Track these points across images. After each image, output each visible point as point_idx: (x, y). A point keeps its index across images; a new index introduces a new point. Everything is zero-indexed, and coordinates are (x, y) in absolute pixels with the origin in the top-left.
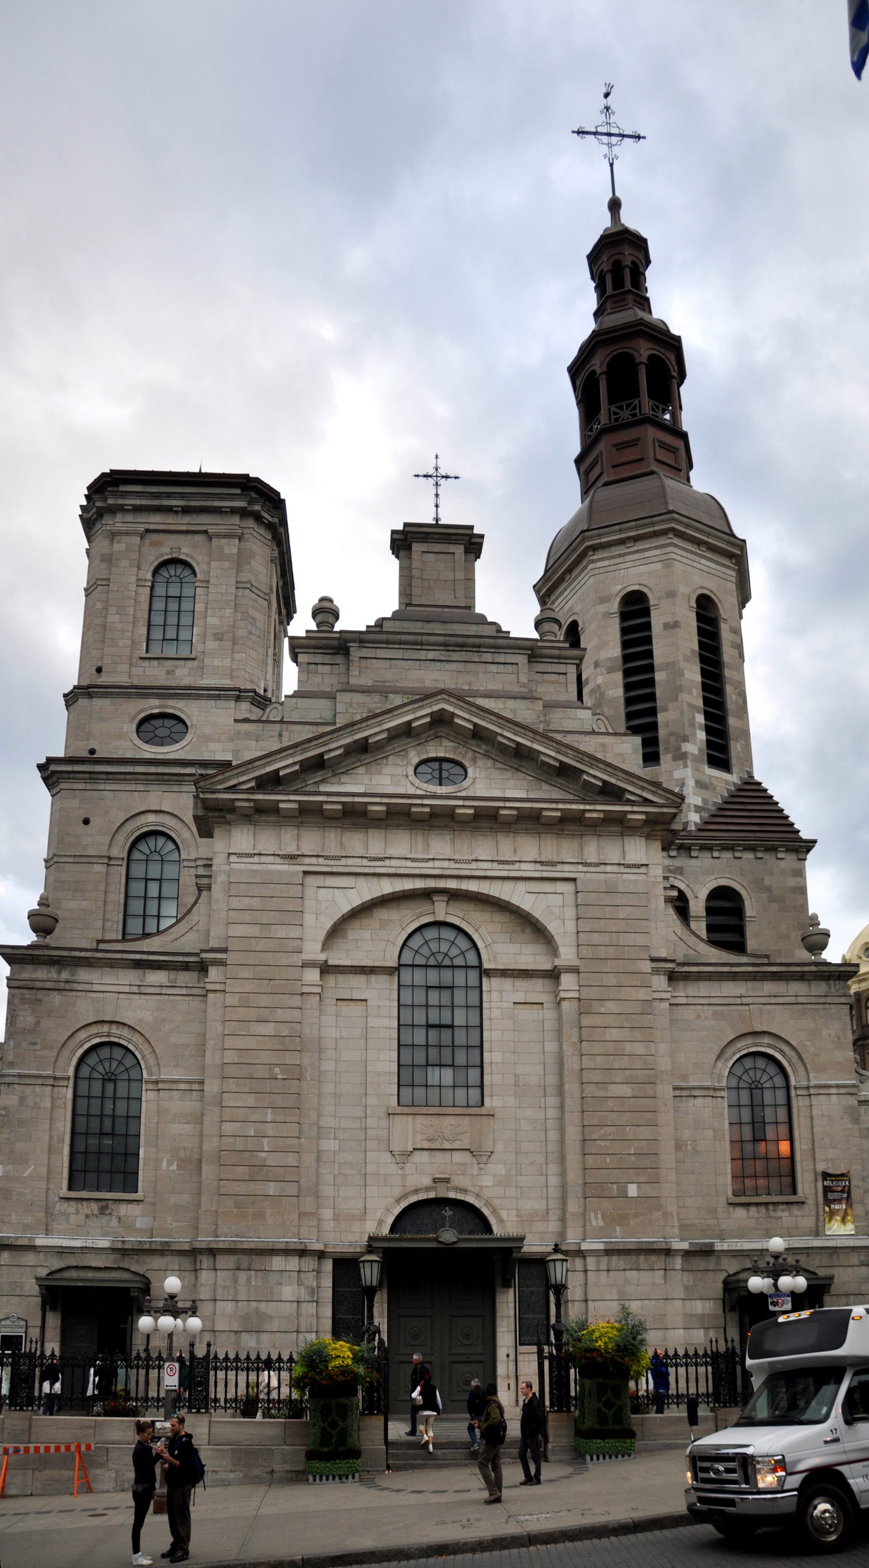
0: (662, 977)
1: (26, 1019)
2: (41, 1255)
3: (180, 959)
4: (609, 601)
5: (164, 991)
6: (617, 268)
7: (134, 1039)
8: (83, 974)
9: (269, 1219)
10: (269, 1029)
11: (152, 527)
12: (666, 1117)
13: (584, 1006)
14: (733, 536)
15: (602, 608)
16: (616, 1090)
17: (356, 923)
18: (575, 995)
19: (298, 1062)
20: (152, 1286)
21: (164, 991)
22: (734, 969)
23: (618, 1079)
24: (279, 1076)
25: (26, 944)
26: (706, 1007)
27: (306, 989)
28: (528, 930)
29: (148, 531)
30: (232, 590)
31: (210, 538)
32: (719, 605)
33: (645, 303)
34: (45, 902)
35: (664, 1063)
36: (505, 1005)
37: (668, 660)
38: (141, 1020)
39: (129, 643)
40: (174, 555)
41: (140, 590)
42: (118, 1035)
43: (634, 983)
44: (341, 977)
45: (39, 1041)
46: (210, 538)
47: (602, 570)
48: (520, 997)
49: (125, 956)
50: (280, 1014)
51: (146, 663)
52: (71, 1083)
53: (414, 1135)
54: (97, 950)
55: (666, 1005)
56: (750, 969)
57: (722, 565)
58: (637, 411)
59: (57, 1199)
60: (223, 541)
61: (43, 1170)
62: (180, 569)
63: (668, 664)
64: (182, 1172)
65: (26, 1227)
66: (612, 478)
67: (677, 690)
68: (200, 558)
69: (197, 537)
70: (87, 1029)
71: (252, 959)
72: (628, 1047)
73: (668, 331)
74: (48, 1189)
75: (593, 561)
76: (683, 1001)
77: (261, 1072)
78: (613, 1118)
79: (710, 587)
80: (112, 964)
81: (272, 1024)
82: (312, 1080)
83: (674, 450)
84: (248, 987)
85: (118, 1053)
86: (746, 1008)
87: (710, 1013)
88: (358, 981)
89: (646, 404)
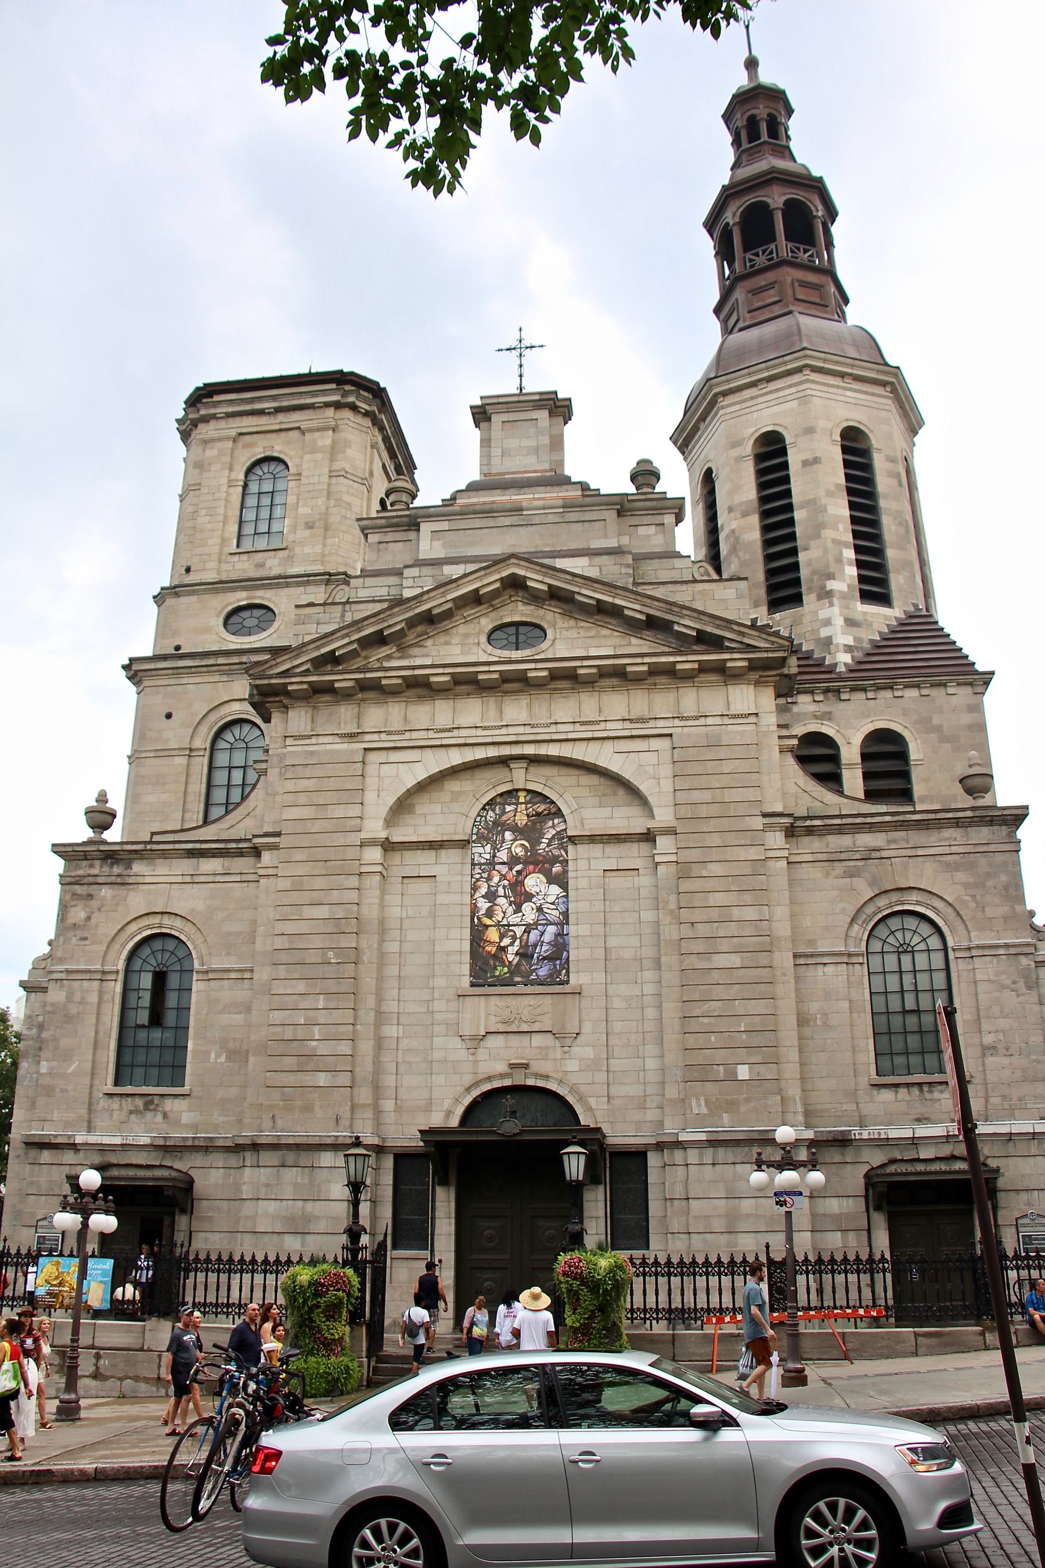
0: (778, 833)
2: (81, 1154)
3: (234, 845)
4: (741, 444)
5: (218, 878)
6: (752, 124)
7: (186, 929)
8: (138, 867)
9: (319, 1113)
10: (323, 912)
12: (786, 990)
13: (684, 870)
14: (886, 364)
15: (735, 453)
16: (720, 961)
18: (673, 858)
19: (354, 945)
20: (195, 1185)
21: (218, 878)
22: (869, 820)
23: (724, 949)
24: (332, 961)
25: (80, 841)
27: (364, 869)
30: (325, 479)
31: (303, 433)
32: (870, 435)
33: (785, 152)
34: (103, 798)
35: (782, 928)
36: (594, 873)
37: (808, 498)
38: (193, 910)
39: (218, 541)
40: (268, 454)
41: (232, 489)
42: (169, 925)
43: (743, 842)
44: (407, 854)
45: (89, 936)
46: (303, 433)
47: (732, 415)
49: (177, 846)
50: (335, 896)
51: (236, 558)
52: (121, 977)
53: (486, 1019)
54: (151, 842)
56: (888, 818)
57: (873, 394)
58: (774, 255)
59: (101, 1095)
60: (317, 434)
61: (88, 1066)
62: (273, 465)
63: (808, 502)
64: (230, 1064)
65: (67, 1124)
66: (748, 323)
67: (818, 528)
68: (292, 453)
70: (138, 921)
71: (305, 841)
72: (736, 913)
73: (810, 174)
74: (92, 1086)
75: (723, 408)
76: (809, 858)
77: (313, 957)
78: (719, 992)
79: (857, 418)
80: (165, 855)
81: (327, 907)
82: (370, 963)
83: (818, 287)
84: (301, 869)
85: (171, 945)
86: (888, 862)
89: (783, 246)
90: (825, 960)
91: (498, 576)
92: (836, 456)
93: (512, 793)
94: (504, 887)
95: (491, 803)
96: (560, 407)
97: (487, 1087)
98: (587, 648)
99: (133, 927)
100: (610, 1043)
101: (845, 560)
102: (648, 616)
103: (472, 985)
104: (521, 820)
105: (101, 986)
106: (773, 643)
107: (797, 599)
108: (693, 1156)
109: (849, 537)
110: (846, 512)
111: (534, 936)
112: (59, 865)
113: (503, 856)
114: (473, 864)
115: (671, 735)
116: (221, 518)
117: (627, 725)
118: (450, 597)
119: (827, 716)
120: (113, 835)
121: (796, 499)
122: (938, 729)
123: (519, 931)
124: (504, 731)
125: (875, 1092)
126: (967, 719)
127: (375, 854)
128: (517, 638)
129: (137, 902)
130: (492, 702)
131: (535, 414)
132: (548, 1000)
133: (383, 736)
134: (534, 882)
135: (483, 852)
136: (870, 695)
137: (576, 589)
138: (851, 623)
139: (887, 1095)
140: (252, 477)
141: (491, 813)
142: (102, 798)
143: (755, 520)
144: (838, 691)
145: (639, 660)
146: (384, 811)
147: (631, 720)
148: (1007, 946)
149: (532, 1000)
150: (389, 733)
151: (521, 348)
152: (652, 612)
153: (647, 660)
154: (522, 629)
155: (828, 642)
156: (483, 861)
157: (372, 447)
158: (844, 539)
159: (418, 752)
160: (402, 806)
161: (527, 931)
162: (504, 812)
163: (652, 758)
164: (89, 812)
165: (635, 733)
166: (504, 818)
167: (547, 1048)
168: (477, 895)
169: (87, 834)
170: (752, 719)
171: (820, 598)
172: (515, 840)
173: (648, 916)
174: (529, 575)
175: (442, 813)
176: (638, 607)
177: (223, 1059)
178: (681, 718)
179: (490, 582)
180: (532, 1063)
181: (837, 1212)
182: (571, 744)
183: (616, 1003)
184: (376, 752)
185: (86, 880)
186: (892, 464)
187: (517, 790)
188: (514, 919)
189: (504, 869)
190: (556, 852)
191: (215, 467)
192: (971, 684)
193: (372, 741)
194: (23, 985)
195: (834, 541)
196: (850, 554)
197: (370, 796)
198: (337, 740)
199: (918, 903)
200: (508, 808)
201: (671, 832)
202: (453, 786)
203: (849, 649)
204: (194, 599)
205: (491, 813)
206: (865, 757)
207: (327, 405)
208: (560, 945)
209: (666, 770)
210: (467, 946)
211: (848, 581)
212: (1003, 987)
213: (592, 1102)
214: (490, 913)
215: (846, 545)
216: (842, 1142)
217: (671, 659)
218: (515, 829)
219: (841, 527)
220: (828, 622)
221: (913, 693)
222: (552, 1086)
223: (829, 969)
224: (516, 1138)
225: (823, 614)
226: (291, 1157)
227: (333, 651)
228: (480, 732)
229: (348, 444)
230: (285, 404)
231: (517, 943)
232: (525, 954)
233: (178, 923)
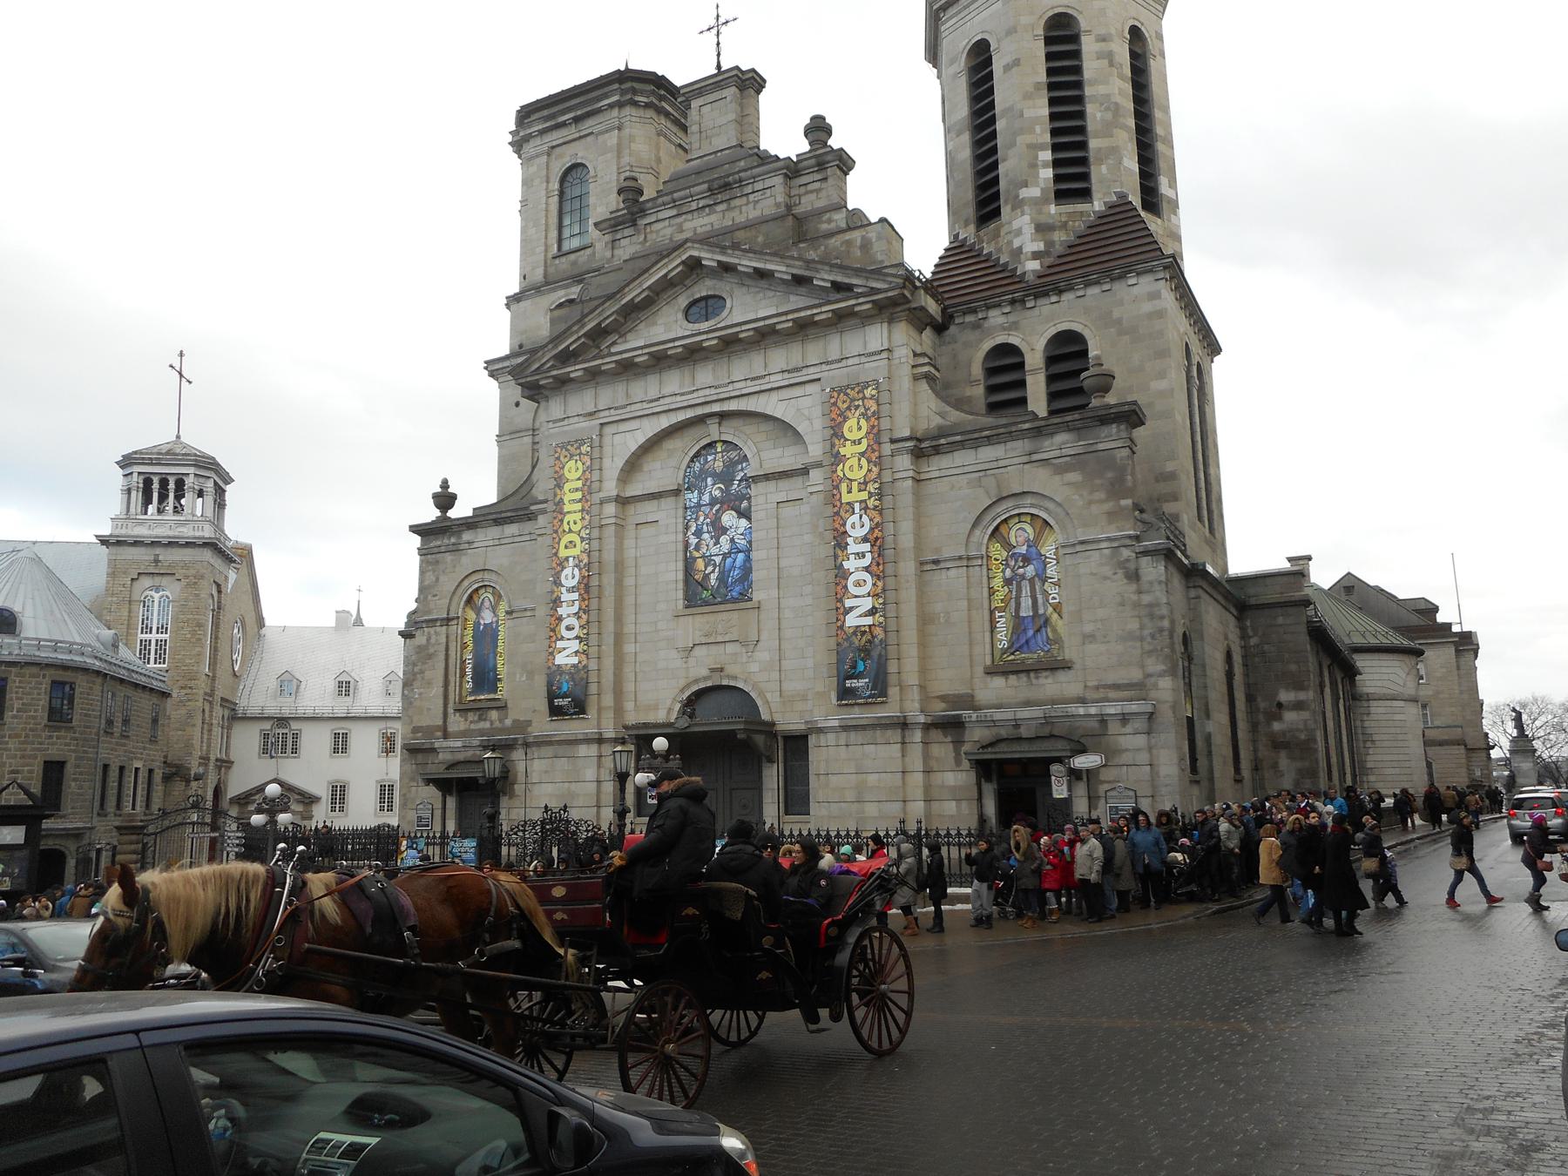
1: (430, 577)
8: (467, 536)
11: (554, 143)
17: (649, 457)
18: (820, 488)
26: (960, 477)
28: (790, 434)
29: (553, 147)
36: (769, 506)
37: (1007, 105)
40: (573, 162)
44: (639, 505)
48: (782, 497)
55: (910, 482)
60: (607, 135)
63: (1010, 109)
69: (589, 139)
76: (936, 474)
87: (965, 481)
88: (650, 506)
90: (948, 565)
91: (679, 261)
92: (1040, 49)
93: (711, 445)
94: (707, 524)
95: (697, 455)
96: (747, 80)
97: (695, 688)
98: (756, 312)
99: (466, 583)
100: (782, 647)
101: (1039, 163)
102: (793, 275)
103: (687, 607)
104: (719, 465)
105: (447, 630)
106: (891, 282)
107: (996, 213)
108: (831, 737)
109: (1047, 138)
110: (1045, 111)
111: (729, 561)
112: (416, 540)
113: (706, 499)
114: (686, 508)
115: (819, 379)
116: (543, 227)
117: (786, 375)
118: (645, 286)
119: (1014, 326)
120: (453, 513)
122: (1119, 321)
123: (718, 559)
124: (695, 395)
125: (988, 679)
126: (1147, 307)
127: (610, 509)
128: (707, 311)
129: (467, 562)
130: (687, 371)
131: (725, 93)
132: (735, 615)
133: (612, 411)
134: (728, 518)
135: (693, 497)
136: (1054, 299)
137: (736, 261)
138: (1042, 229)
139: (999, 682)
140: (567, 184)
141: (697, 464)
142: (445, 484)
144: (1023, 302)
145: (784, 318)
146: (616, 473)
147: (789, 371)
148: (1109, 539)
149: (724, 616)
150: (616, 408)
151: (718, 26)
152: (795, 271)
153: (790, 317)
154: (711, 302)
155: (1020, 248)
156: (692, 505)
157: (659, 135)
158: (1040, 141)
159: (638, 421)
160: (632, 466)
161: (724, 559)
162: (706, 462)
163: (806, 402)
164: (436, 496)
165: (792, 381)
166: (707, 467)
167: (736, 654)
168: (689, 533)
169: (438, 513)
170: (884, 355)
171: (1013, 209)
172: (713, 485)
173: (807, 538)
174: (703, 255)
175: (662, 468)
176: (784, 269)
177: (524, 679)
178: (827, 363)
179: (672, 266)
180: (726, 667)
181: (952, 784)
182: (745, 398)
183: (787, 614)
184: (612, 425)
185: (436, 550)
186: (1103, 44)
187: (716, 442)
188: (714, 550)
189: (707, 509)
190: (744, 492)
191: (537, 182)
192: (1151, 271)
193: (605, 417)
194: (401, 634)
196: (1047, 155)
197: (607, 462)
198: (582, 419)
199: (1032, 506)
200: (710, 458)
201: (819, 465)
202: (672, 444)
203: (1036, 255)
204: (529, 302)
205: (697, 464)
206: (1051, 360)
207: (611, 106)
208: (747, 569)
209: (817, 411)
210: (681, 576)
211: (1042, 185)
212: (1106, 578)
213: (769, 696)
214: (697, 548)
215: (1042, 147)
217: (809, 312)
218: (715, 475)
219: (1038, 129)
220: (1019, 232)
221: (1094, 291)
222: (740, 685)
223: (952, 573)
224: (688, 730)
225: (1016, 225)
226: (561, 750)
227: (568, 346)
228: (679, 398)
229: (632, 138)
230: (579, 113)
231: (717, 570)
232: (722, 579)
233: (494, 577)
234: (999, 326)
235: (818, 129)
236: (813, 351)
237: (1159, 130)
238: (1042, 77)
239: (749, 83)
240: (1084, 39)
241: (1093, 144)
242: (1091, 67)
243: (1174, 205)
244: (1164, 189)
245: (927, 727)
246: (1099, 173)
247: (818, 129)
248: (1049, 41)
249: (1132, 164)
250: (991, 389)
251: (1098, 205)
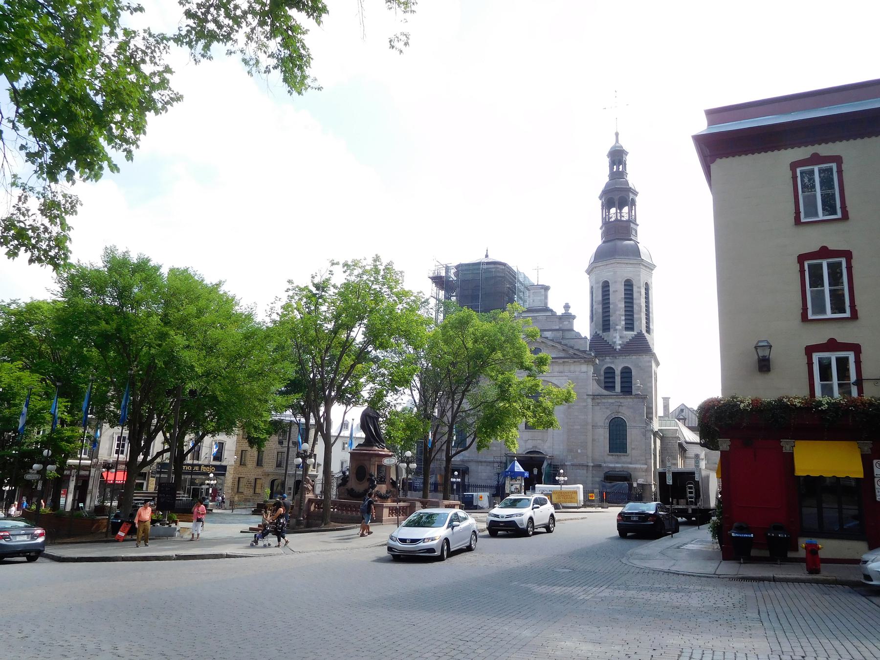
16: (576, 427)
35: (590, 421)
92: (622, 288)
107: (609, 329)
109: (623, 313)
119: (613, 363)
121: (611, 301)
126: (647, 364)
138: (621, 337)
139: (611, 457)
143: (601, 306)
155: (615, 342)
195: (620, 315)
196: (623, 318)
203: (620, 345)
206: (622, 373)
216: (600, 466)
225: (614, 335)
234: (609, 362)
235: (567, 307)
236: (566, 368)
237: (650, 310)
238: (623, 296)
239: (546, 288)
240: (634, 287)
241: (635, 316)
242: (635, 295)
243: (653, 330)
244: (651, 327)
245: (593, 466)
246: (636, 324)
247: (567, 307)
248: (625, 285)
249: (644, 321)
250: (605, 378)
251: (635, 333)
